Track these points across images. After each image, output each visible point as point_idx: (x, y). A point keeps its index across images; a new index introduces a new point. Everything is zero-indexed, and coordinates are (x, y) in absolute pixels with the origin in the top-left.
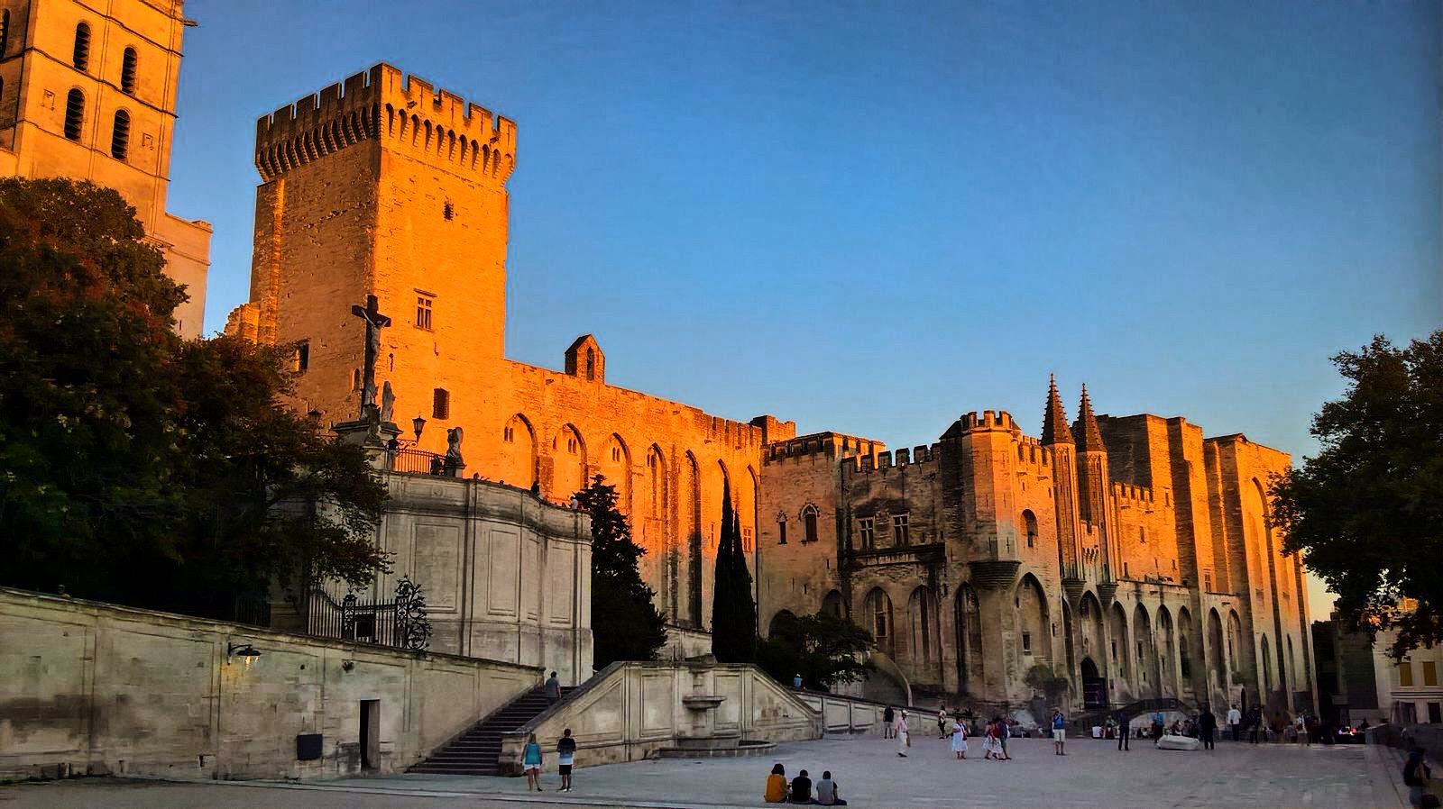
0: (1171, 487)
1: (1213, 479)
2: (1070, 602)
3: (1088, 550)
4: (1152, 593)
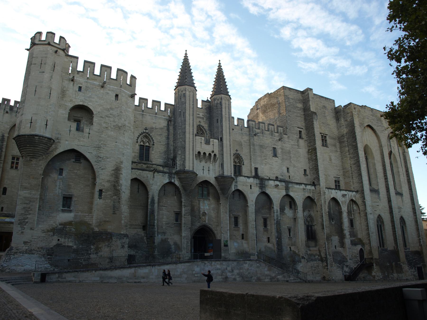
0: (304, 128)
1: (340, 127)
2: (183, 186)
3: (204, 153)
4: (277, 186)
